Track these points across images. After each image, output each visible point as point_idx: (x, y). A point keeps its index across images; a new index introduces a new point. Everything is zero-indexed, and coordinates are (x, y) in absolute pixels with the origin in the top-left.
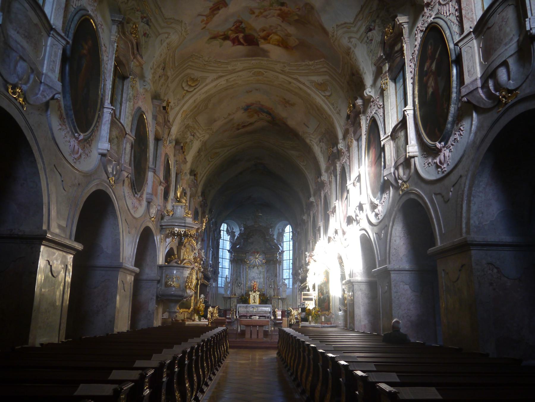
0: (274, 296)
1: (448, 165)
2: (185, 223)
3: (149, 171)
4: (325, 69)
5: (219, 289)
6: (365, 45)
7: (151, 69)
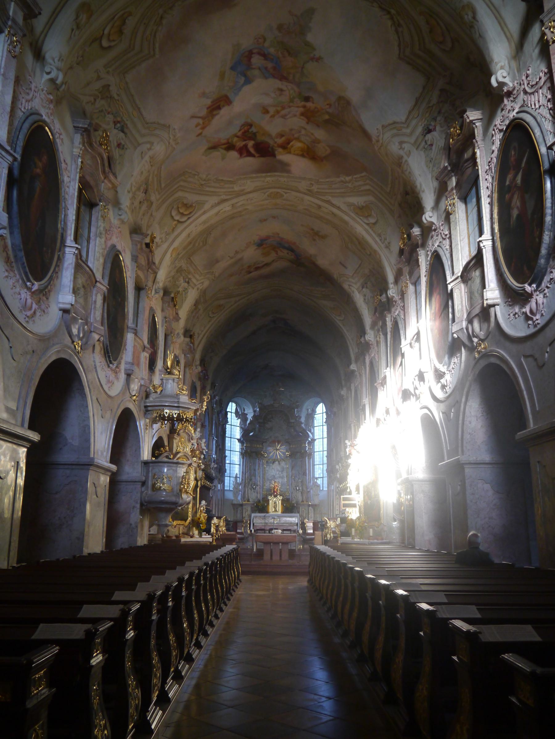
0: (303, 501)
1: (542, 315)
2: (178, 402)
3: (128, 332)
4: (367, 187)
5: (226, 493)
6: (422, 153)
7: (129, 192)
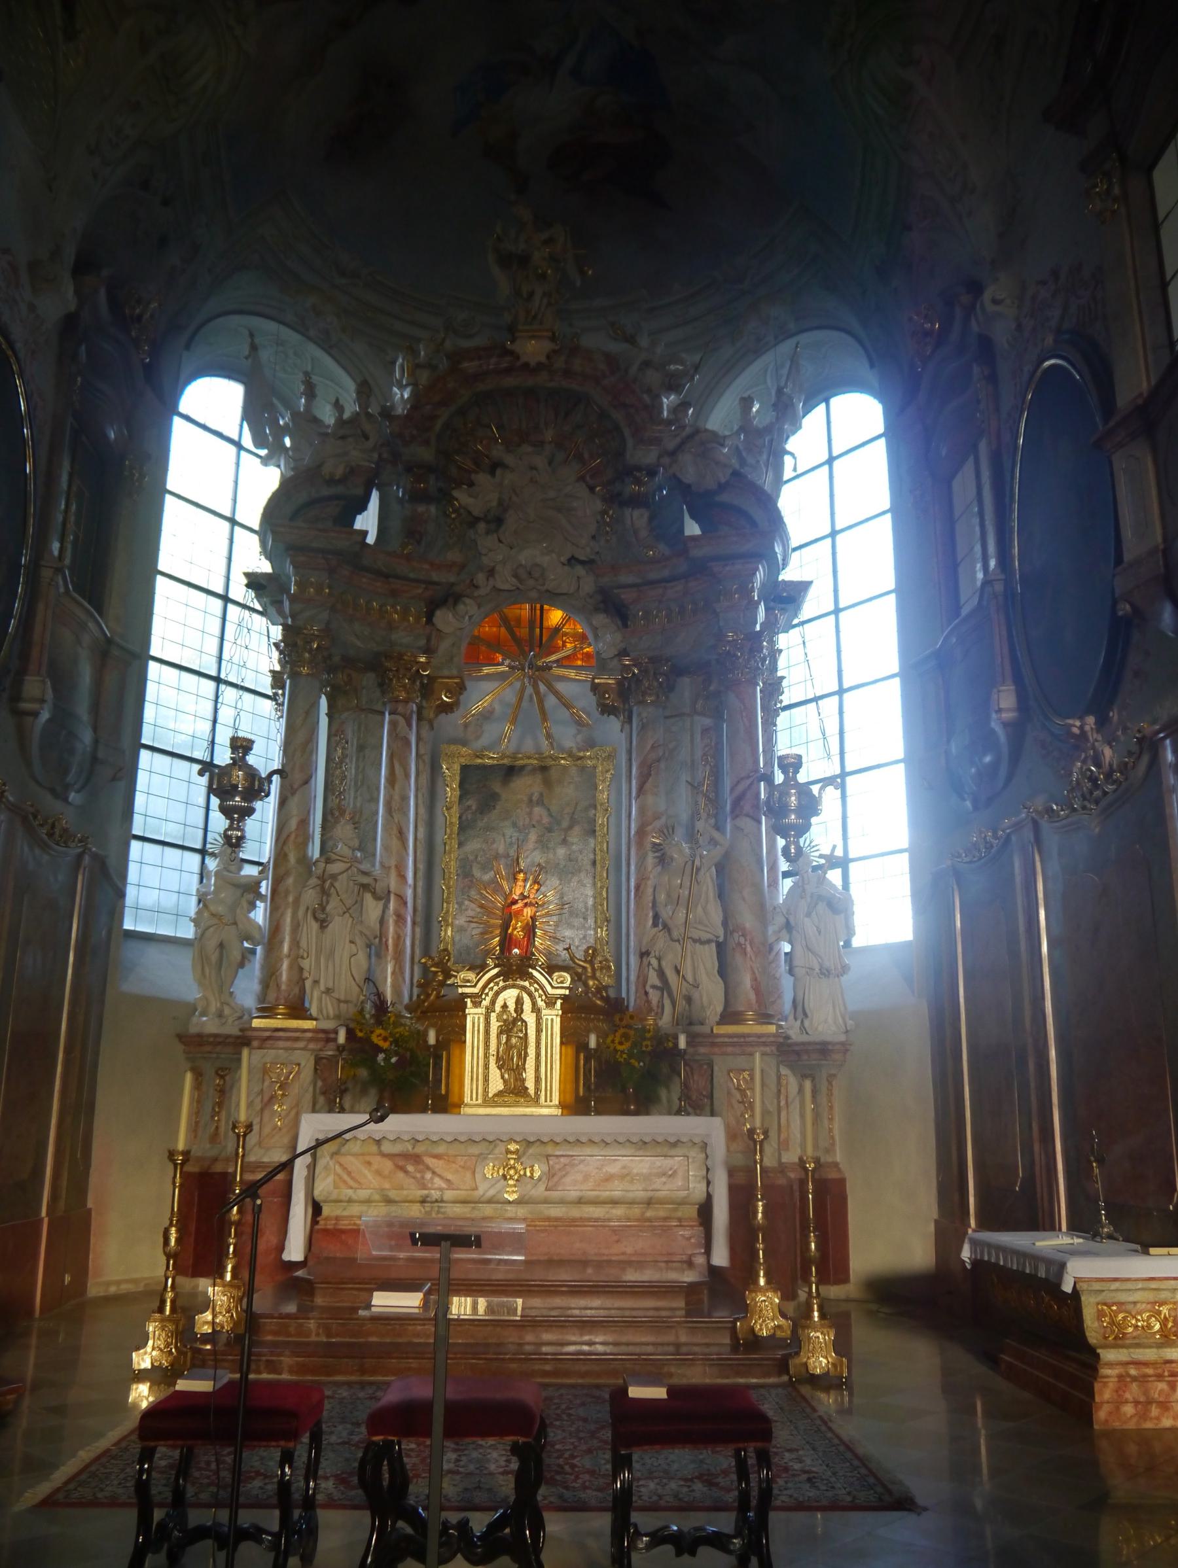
0: (730, 1016)
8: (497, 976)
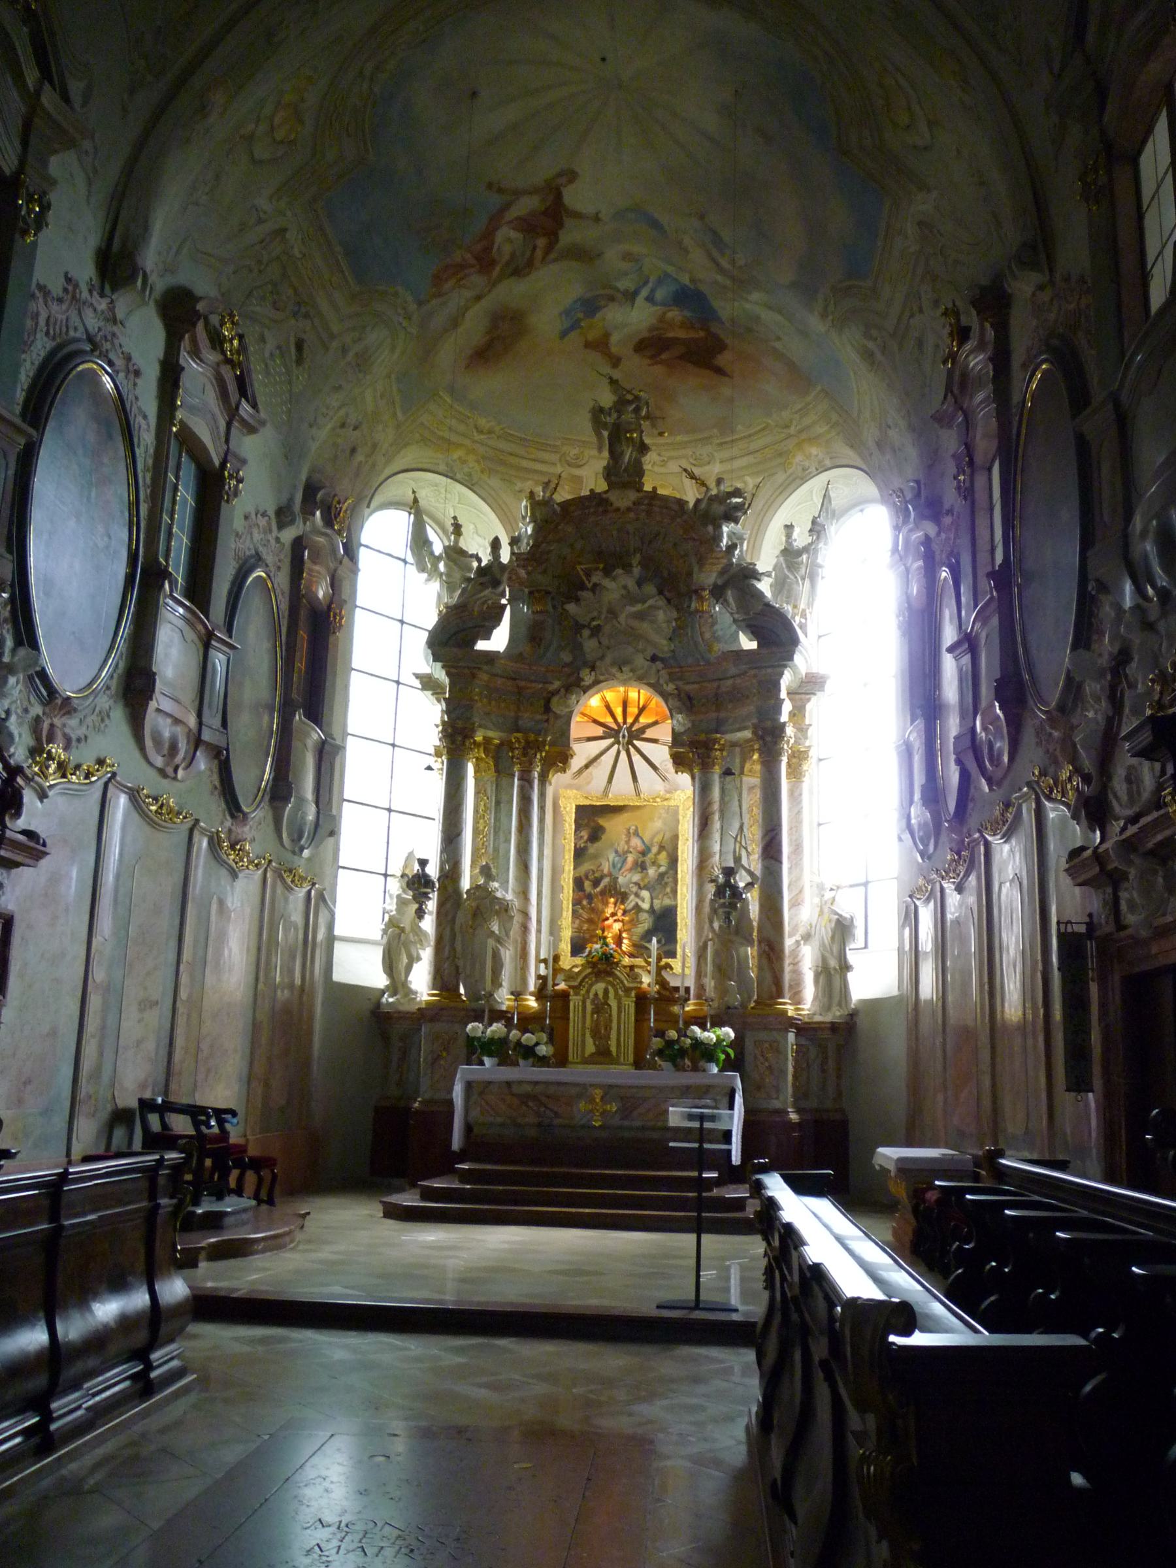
8: (589, 974)
